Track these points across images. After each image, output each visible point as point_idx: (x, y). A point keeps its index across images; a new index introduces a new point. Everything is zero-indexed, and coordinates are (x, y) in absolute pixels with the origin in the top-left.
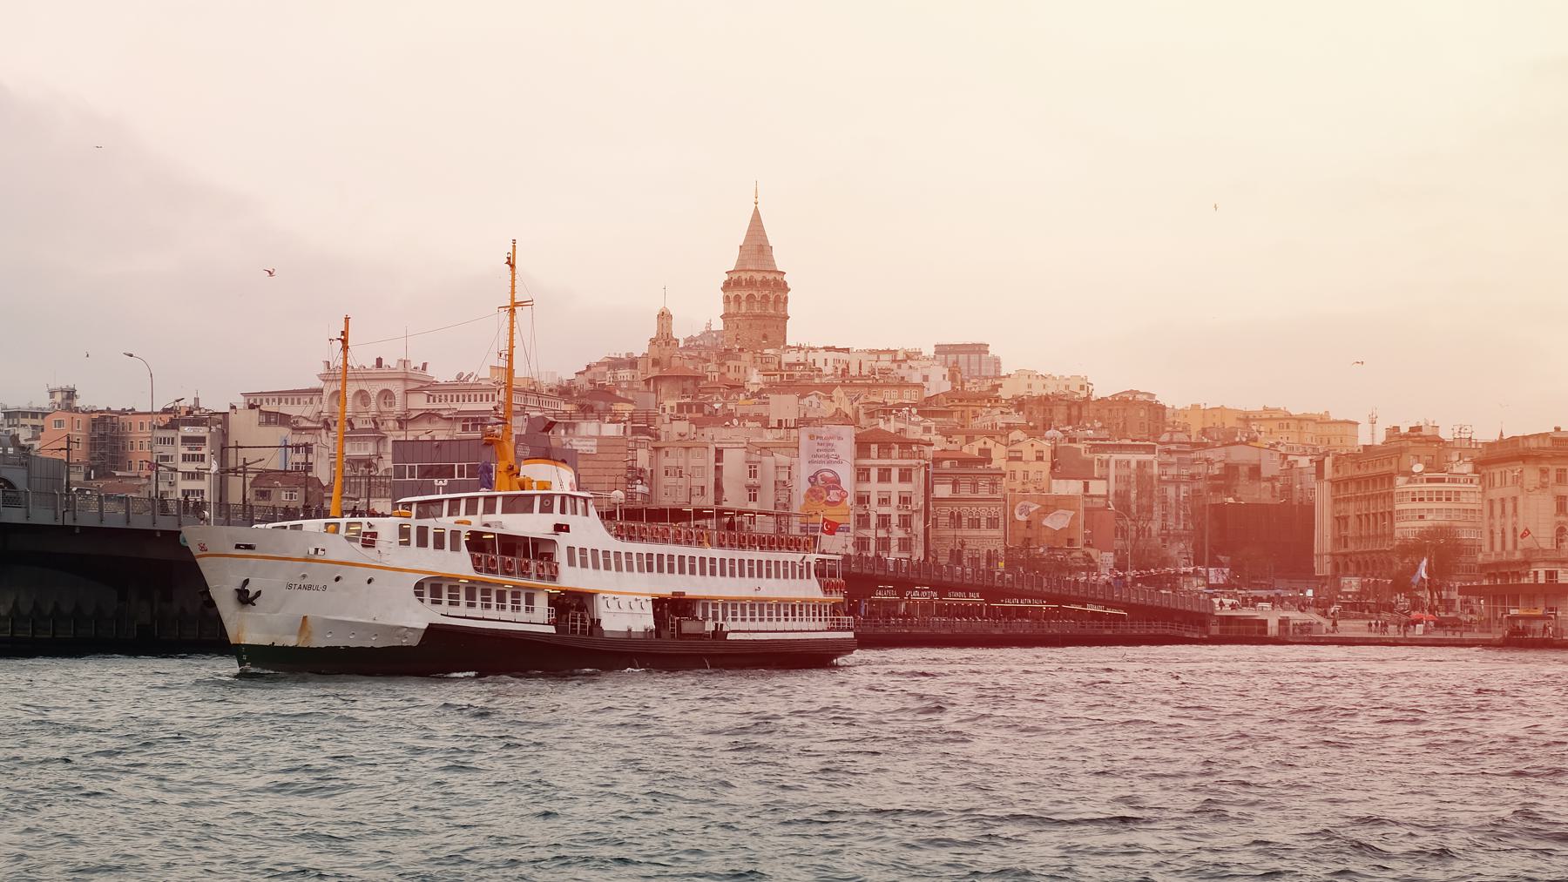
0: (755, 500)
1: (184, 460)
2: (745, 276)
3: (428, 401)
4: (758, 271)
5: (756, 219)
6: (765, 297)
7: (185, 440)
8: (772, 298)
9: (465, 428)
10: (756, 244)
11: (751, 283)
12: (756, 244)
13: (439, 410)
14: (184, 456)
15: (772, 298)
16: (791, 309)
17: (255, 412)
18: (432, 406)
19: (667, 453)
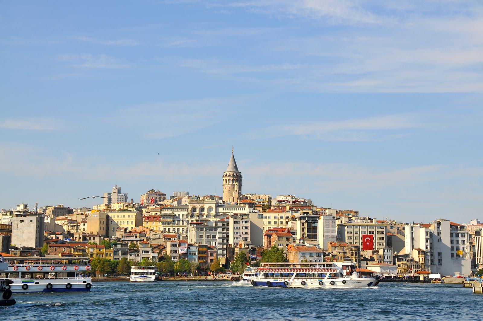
3: (223, 210)
4: (232, 172)
13: (227, 213)
17: (257, 214)
18: (224, 211)
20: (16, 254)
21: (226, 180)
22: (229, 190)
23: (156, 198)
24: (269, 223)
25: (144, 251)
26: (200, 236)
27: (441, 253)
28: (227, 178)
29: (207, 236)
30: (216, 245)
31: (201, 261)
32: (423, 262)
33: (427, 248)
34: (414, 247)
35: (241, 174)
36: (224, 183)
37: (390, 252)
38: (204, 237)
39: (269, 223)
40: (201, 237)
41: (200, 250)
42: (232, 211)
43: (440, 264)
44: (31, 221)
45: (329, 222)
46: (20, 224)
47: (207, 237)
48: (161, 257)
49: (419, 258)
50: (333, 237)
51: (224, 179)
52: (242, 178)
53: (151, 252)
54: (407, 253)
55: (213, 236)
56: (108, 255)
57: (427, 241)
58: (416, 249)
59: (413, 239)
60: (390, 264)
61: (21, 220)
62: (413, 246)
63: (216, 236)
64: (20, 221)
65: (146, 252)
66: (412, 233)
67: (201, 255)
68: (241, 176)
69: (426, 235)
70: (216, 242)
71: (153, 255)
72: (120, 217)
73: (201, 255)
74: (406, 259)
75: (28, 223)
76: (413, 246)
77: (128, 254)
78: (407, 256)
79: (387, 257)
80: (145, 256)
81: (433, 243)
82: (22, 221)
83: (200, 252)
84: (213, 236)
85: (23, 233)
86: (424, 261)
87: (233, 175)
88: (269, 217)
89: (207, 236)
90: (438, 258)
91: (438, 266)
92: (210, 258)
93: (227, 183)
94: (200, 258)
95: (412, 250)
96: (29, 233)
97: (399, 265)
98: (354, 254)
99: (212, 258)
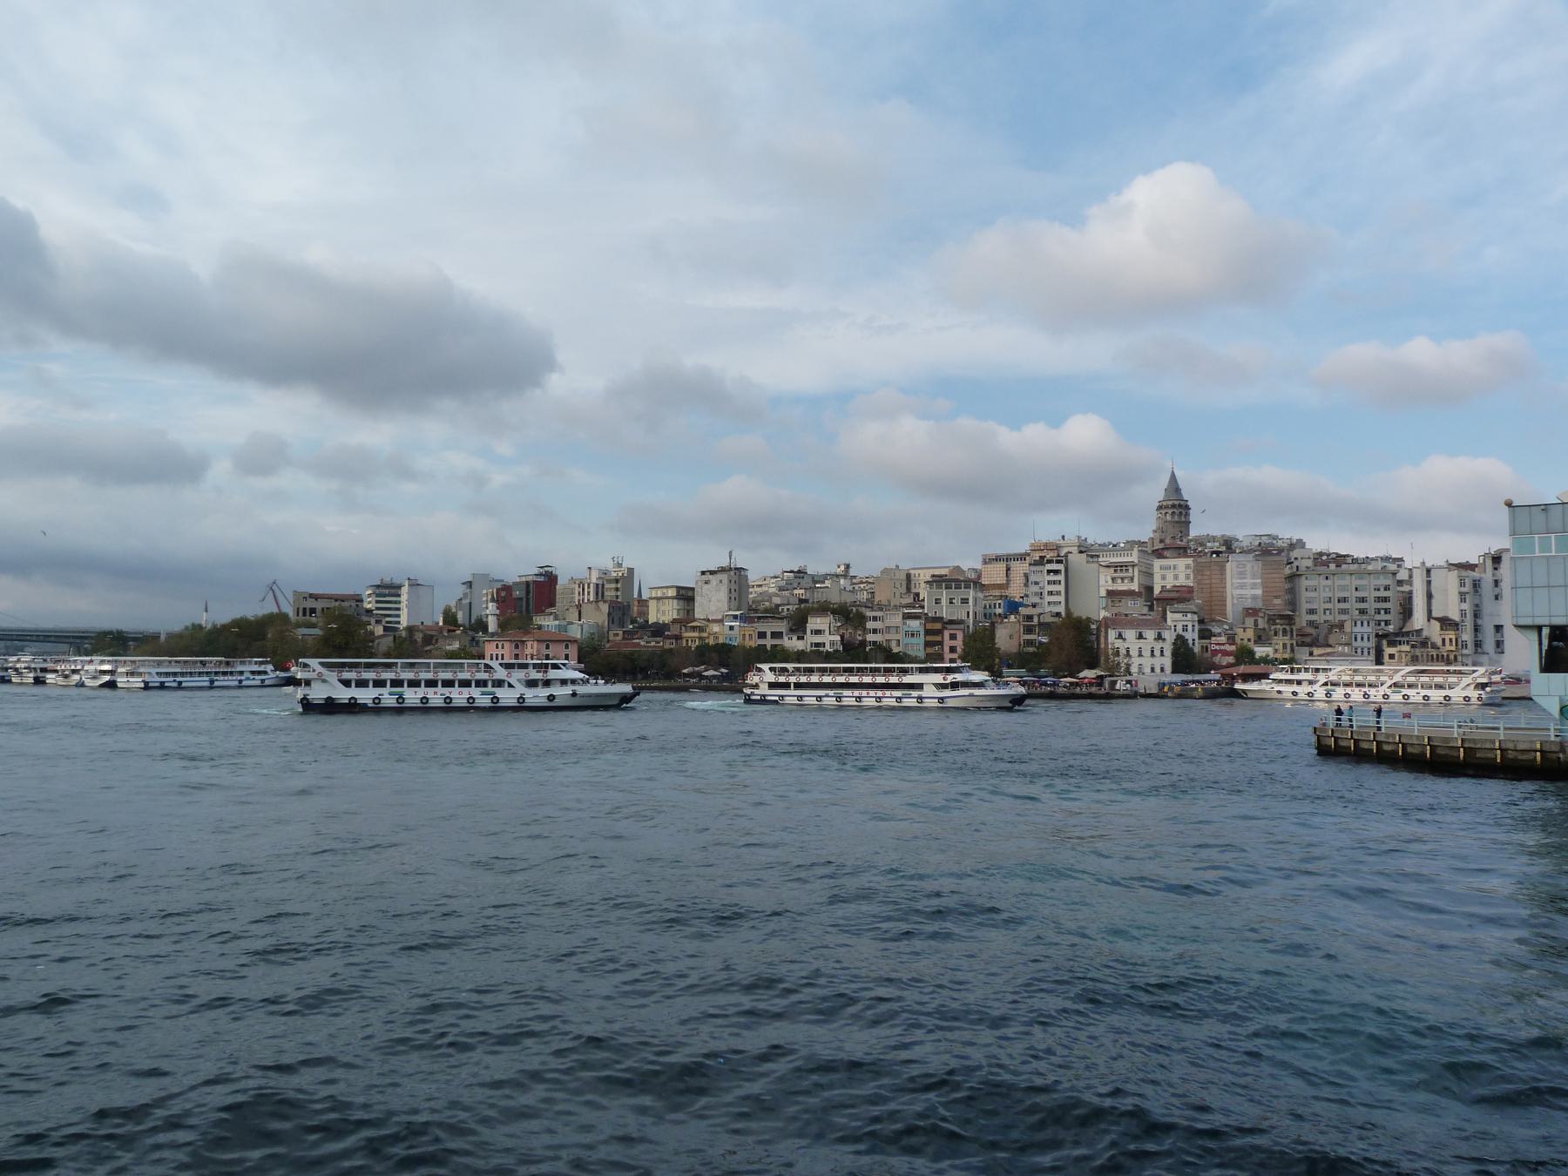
0: (1465, 602)
1: (1049, 584)
2: (1170, 503)
5: (1173, 472)
6: (1181, 512)
7: (1049, 572)
8: (1184, 512)
9: (1116, 571)
10: (1174, 487)
11: (1167, 507)
12: (1174, 487)
14: (1048, 581)
15: (1184, 512)
16: (1192, 518)
17: (1084, 555)
19: (1306, 578)
20: (617, 635)
24: (1176, 577)
25: (815, 631)
26: (936, 599)
27: (1502, 626)
29: (951, 599)
30: (968, 617)
31: (930, 650)
32: (1453, 648)
33: (1463, 613)
34: (1435, 614)
35: (1189, 503)
37: (1368, 625)
38: (944, 602)
39: (1176, 577)
40: (938, 601)
41: (927, 628)
42: (1108, 559)
43: (1499, 650)
44: (721, 581)
45: (1244, 566)
47: (951, 603)
48: (729, 645)
49: (1444, 640)
50: (1254, 597)
53: (827, 632)
54: (1417, 627)
55: (962, 599)
56: (747, 637)
57: (1463, 600)
58: (1436, 619)
59: (1430, 596)
60: (1356, 652)
62: (1430, 611)
63: (968, 599)
65: (818, 632)
66: (1429, 583)
67: (930, 638)
68: (1187, 508)
69: (1462, 584)
70: (968, 613)
71: (833, 638)
73: (930, 638)
74: (1408, 641)
75: (717, 585)
76: (1430, 611)
77: (786, 638)
78: (1419, 631)
79: (1362, 639)
80: (818, 639)
81: (1481, 603)
82: (707, 582)
83: (928, 632)
84: (962, 599)
85: (710, 601)
86: (1454, 644)
87: (1173, 506)
88: (1174, 568)
89: (951, 599)
90: (1495, 637)
91: (1495, 656)
92: (948, 643)
94: (927, 644)
95: (1429, 620)
97: (1390, 655)
98: (1281, 633)
99: (953, 643)
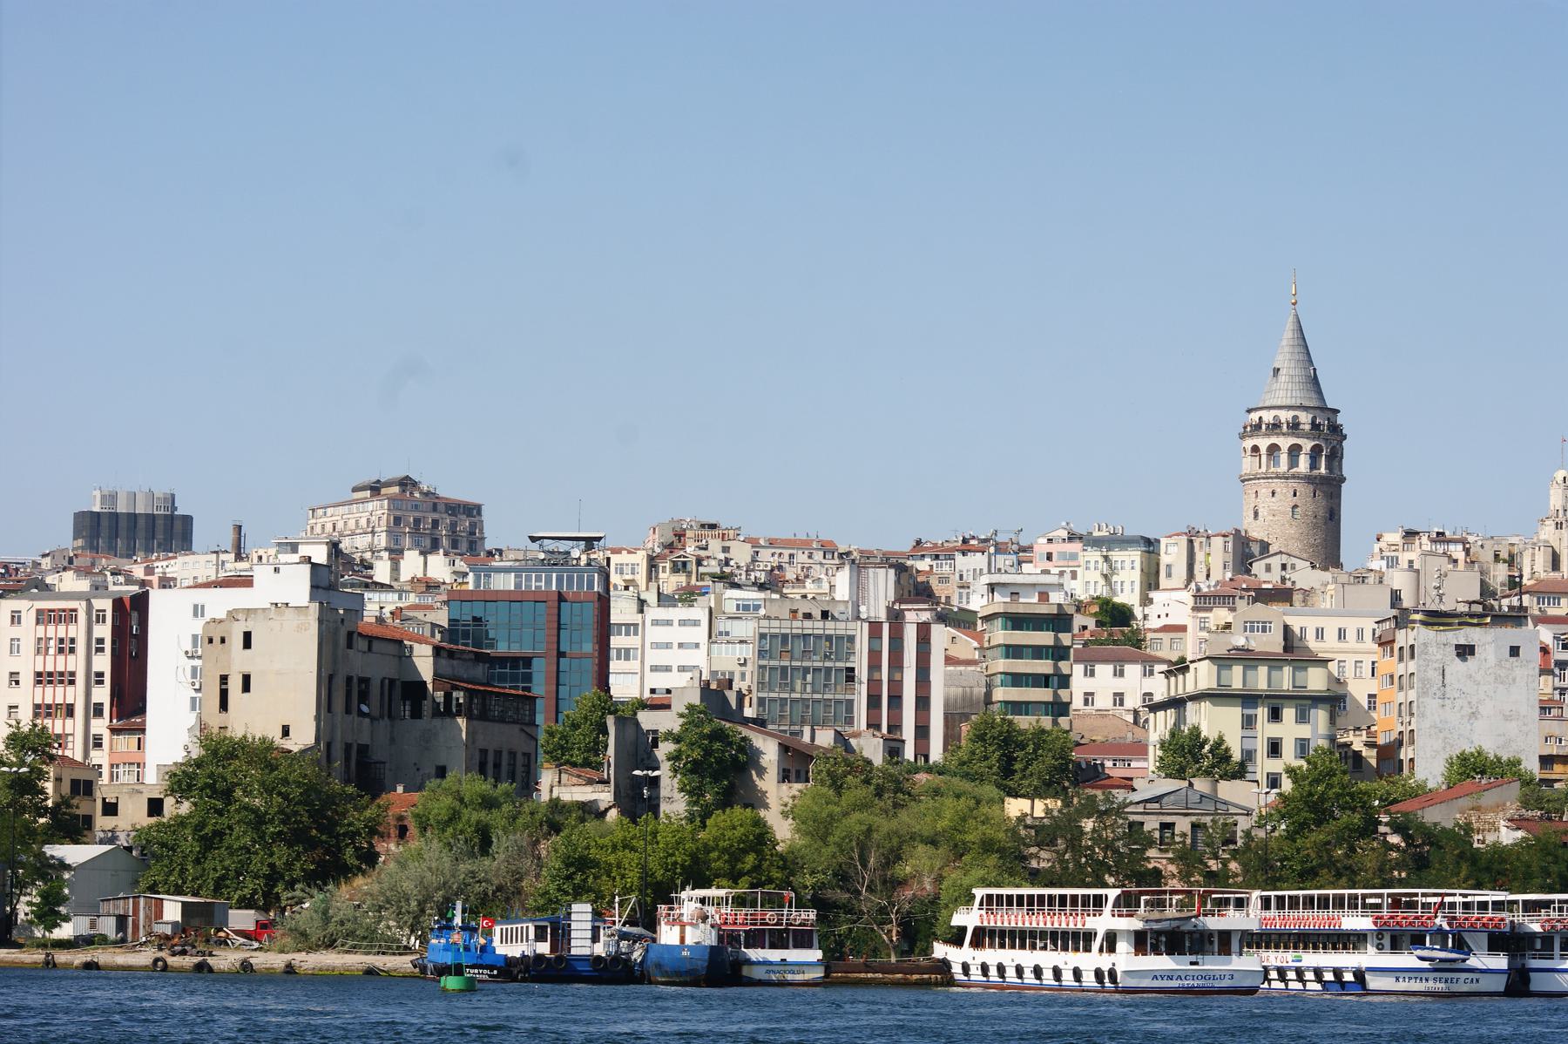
21: (1255, 449)
22: (1295, 506)
23: (435, 523)
28: (1285, 443)
36: (1248, 465)
44: (1515, 651)
46: (1456, 666)
51: (1249, 443)
52: (1344, 443)
61: (1462, 642)
64: (1457, 647)
72: (1351, 635)
75: (1499, 664)
82: (1465, 651)
85: (1474, 715)
87: (1295, 426)
93: (1264, 469)
96: (1507, 718)
